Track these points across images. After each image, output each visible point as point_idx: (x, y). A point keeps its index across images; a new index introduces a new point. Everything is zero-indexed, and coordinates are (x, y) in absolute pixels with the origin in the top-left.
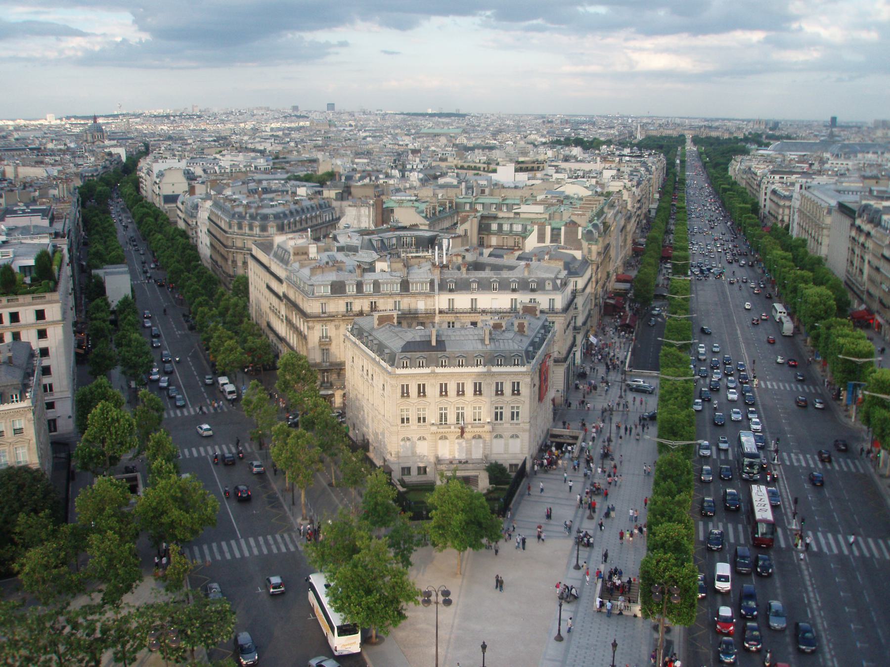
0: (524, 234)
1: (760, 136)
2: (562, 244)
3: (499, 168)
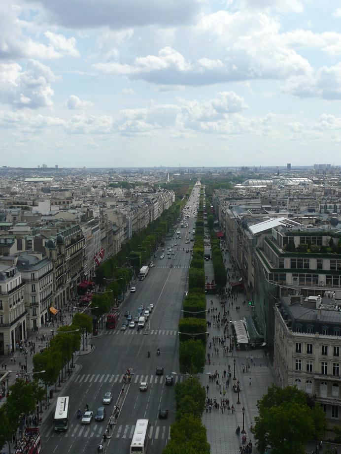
0: (10, 246)
1: (242, 177)
2: (33, 250)
3: (40, 204)
